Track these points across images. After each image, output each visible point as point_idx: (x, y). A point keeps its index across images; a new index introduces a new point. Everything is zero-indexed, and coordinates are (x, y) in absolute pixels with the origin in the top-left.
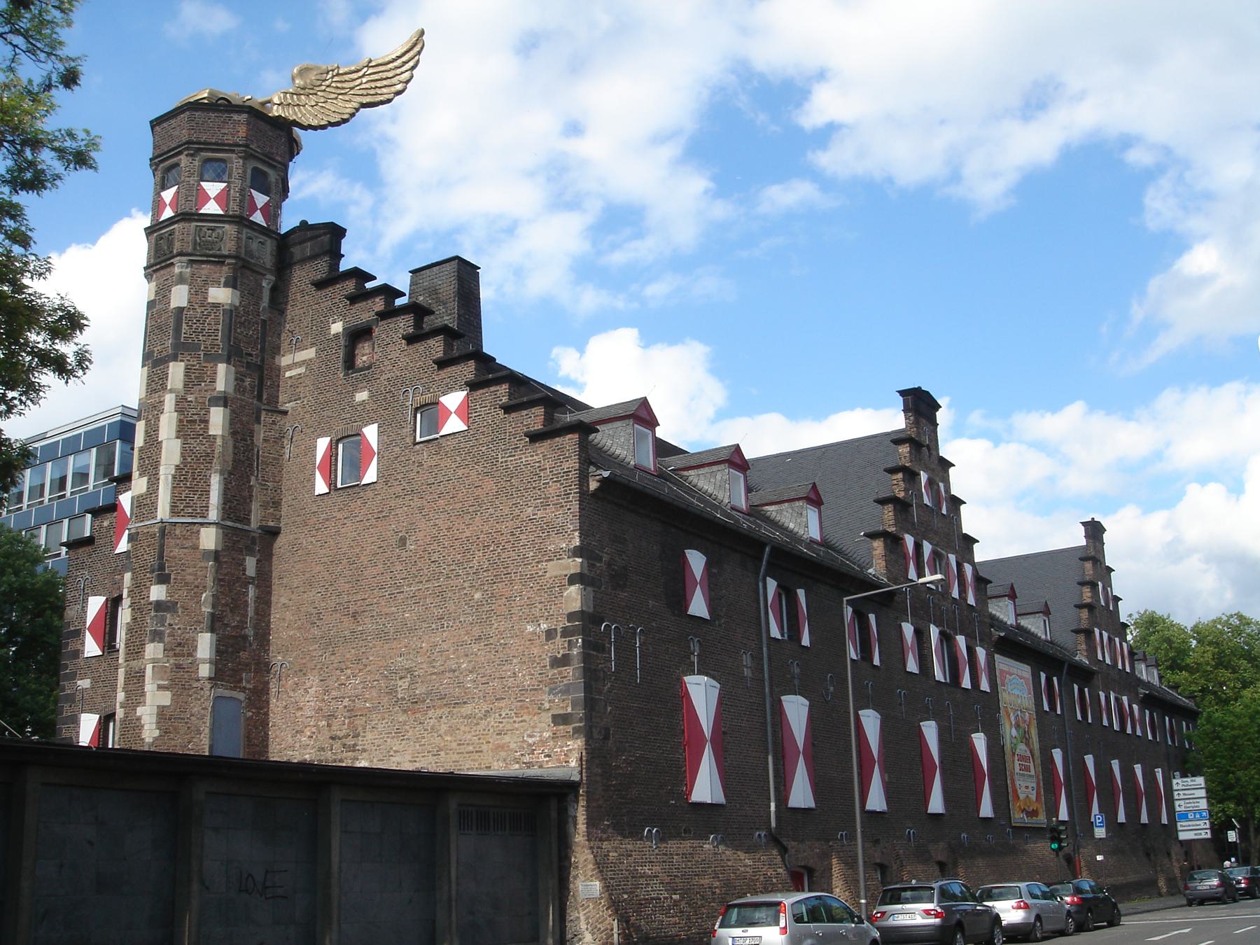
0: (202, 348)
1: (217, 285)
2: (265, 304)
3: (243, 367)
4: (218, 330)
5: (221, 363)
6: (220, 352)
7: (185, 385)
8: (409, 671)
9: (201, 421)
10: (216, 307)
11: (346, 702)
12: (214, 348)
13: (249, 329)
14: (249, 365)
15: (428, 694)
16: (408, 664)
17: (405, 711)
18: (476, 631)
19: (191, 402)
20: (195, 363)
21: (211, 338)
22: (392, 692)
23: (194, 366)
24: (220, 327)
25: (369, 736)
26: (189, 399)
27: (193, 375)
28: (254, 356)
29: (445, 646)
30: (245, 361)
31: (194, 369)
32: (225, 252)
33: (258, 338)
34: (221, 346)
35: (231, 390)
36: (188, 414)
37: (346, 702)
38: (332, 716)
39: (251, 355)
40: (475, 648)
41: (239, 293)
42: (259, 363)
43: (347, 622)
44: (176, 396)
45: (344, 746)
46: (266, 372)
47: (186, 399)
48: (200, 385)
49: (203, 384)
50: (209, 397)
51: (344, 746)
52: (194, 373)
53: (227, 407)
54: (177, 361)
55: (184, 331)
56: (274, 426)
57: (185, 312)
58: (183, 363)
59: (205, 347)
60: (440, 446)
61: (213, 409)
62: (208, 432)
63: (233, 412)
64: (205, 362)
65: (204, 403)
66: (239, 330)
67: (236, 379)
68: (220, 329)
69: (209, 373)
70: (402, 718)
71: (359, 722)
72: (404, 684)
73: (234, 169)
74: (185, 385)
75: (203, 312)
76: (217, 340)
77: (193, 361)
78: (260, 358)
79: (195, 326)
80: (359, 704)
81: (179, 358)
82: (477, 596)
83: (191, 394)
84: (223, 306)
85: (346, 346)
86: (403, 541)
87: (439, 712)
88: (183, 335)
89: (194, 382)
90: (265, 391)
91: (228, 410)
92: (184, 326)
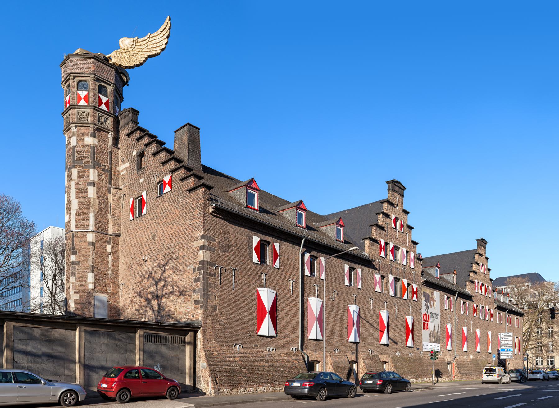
0: (83, 163)
1: (88, 136)
2: (110, 145)
3: (101, 170)
4: (89, 155)
5: (91, 168)
6: (90, 164)
7: (78, 178)
9: (85, 192)
10: (88, 145)
12: (88, 163)
13: (103, 155)
14: (104, 170)
19: (81, 184)
20: (81, 169)
21: (87, 158)
23: (81, 170)
24: (90, 154)
26: (80, 184)
27: (81, 174)
28: (106, 166)
30: (102, 168)
31: (81, 171)
32: (89, 122)
33: (107, 159)
34: (91, 162)
35: (96, 180)
36: (80, 190)
39: (105, 166)
41: (97, 140)
42: (109, 169)
44: (75, 182)
46: (113, 173)
47: (79, 183)
48: (84, 178)
49: (85, 177)
50: (87, 182)
52: (81, 173)
53: (94, 186)
54: (74, 168)
55: (76, 156)
56: (117, 195)
57: (76, 148)
58: (76, 169)
59: (84, 162)
61: (89, 188)
62: (87, 197)
63: (97, 188)
64: (85, 168)
65: (86, 185)
66: (98, 155)
67: (98, 175)
68: (90, 155)
69: (87, 173)
73: (91, 85)
74: (78, 178)
75: (83, 148)
76: (89, 159)
77: (80, 168)
78: (109, 167)
79: (80, 154)
81: (75, 167)
83: (81, 181)
84: (91, 145)
85: (137, 160)
88: (76, 158)
89: (81, 176)
90: (112, 180)
91: (95, 188)
92: (76, 154)
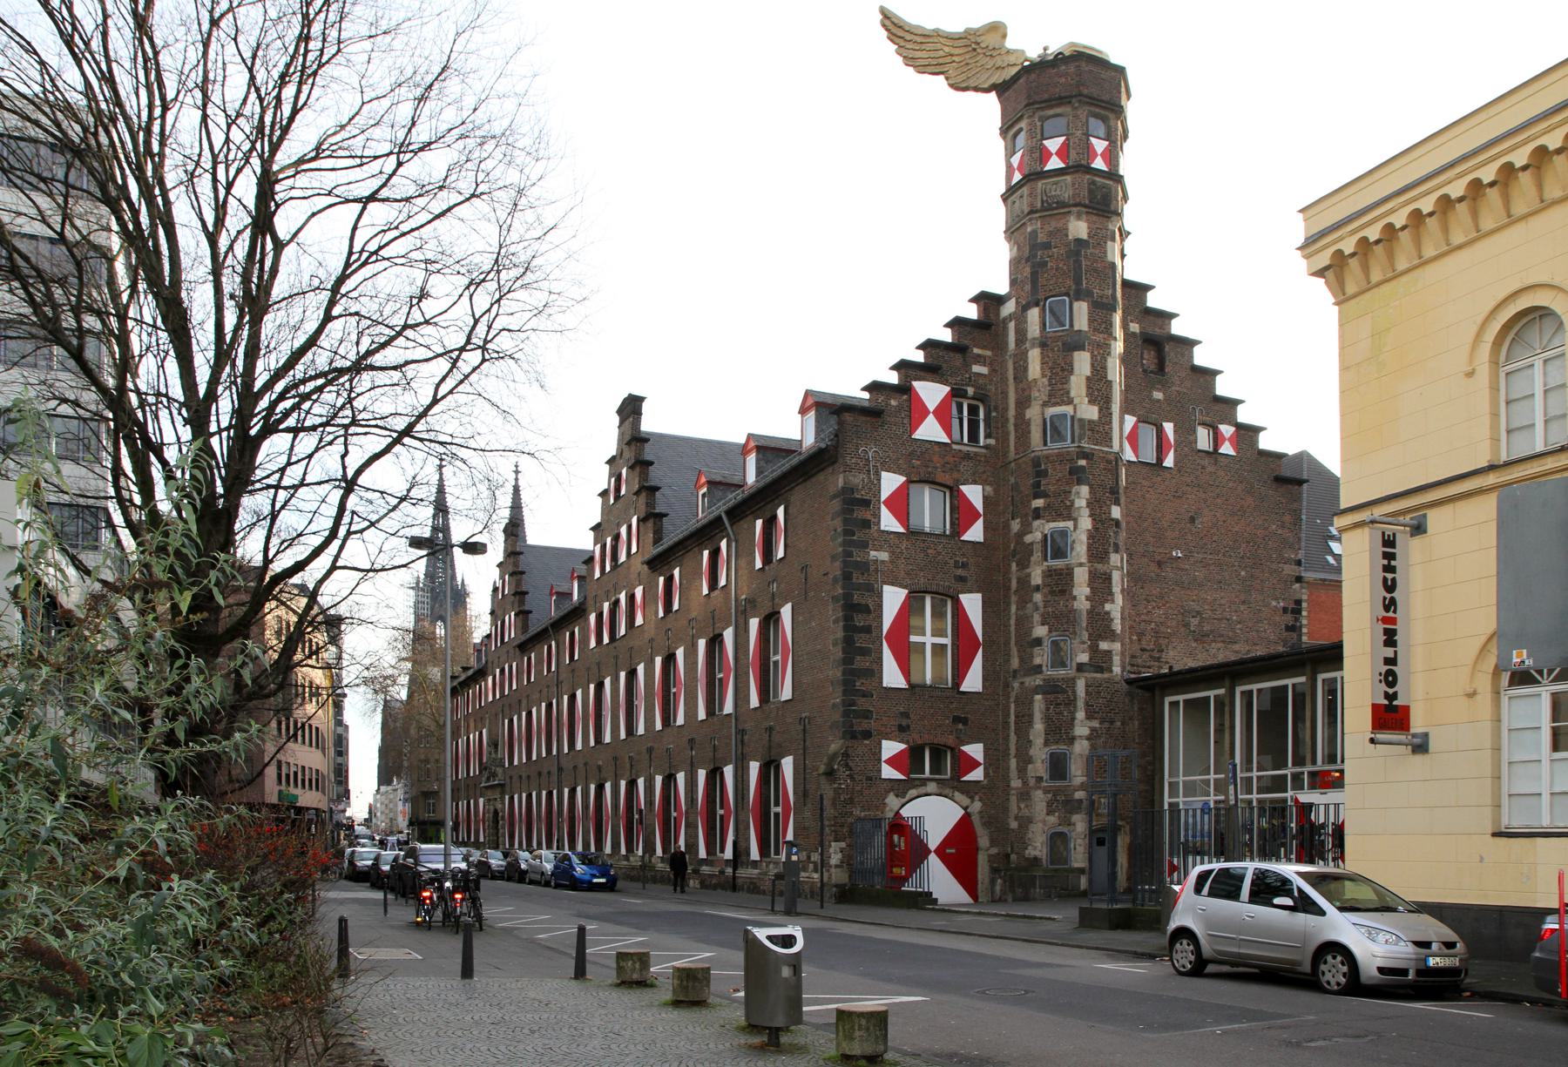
8: (1198, 613)
11: (1153, 625)
15: (1212, 631)
16: (1198, 608)
17: (1196, 640)
18: (1242, 597)
22: (1187, 625)
25: (1171, 653)
29: (1223, 602)
37: (1153, 625)
38: (1141, 635)
40: (1242, 608)
43: (1153, 567)
45: (1151, 657)
51: (1151, 657)
60: (1216, 460)
70: (1194, 645)
71: (1163, 642)
72: (1195, 621)
80: (1163, 629)
82: (1243, 573)
86: (1192, 520)
87: (1220, 645)
